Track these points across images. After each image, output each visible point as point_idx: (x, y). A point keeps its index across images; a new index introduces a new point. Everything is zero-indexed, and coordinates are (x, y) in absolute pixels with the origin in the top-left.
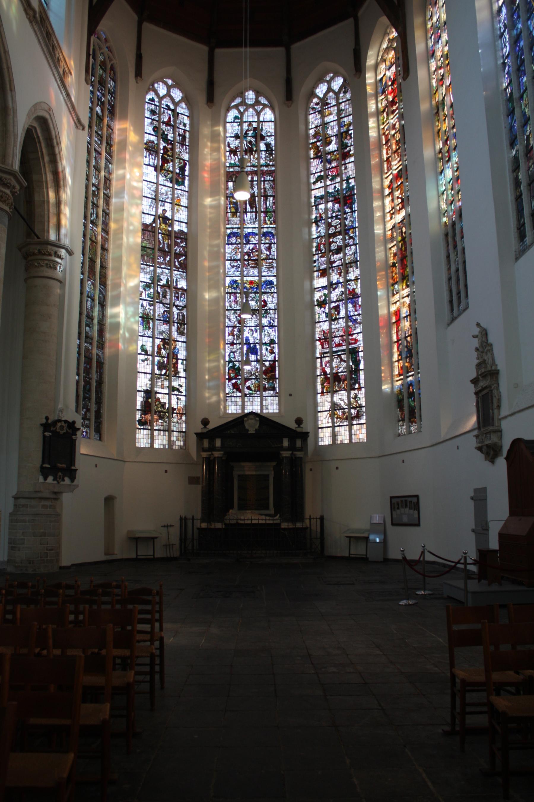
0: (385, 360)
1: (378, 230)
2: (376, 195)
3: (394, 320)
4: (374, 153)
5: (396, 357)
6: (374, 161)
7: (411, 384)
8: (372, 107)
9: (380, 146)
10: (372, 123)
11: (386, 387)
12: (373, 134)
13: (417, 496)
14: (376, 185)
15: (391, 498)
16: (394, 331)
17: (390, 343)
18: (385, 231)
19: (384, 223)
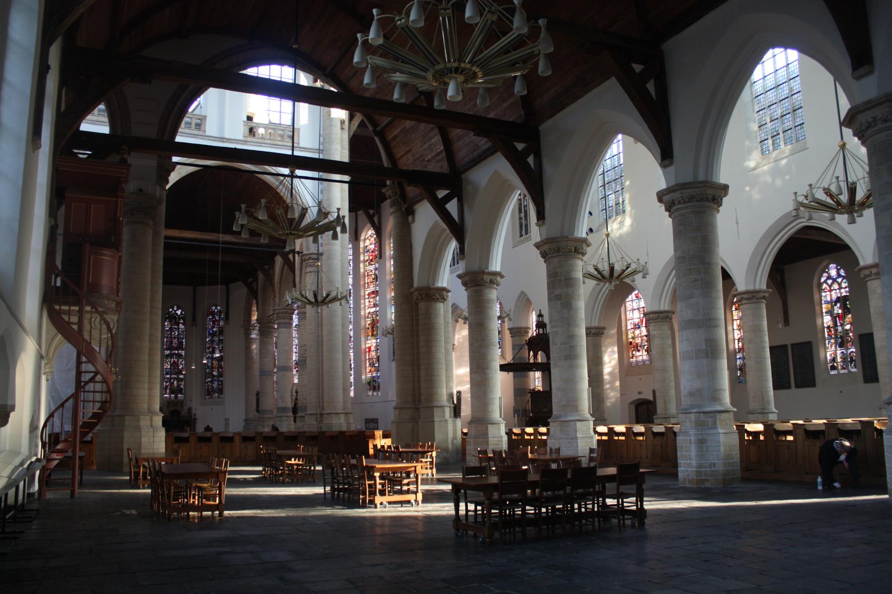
0: (363, 366)
1: (362, 313)
2: (362, 298)
3: (367, 350)
4: (362, 279)
5: (368, 365)
6: (362, 283)
7: (374, 377)
8: (362, 258)
9: (364, 276)
10: (362, 265)
11: (363, 377)
12: (362, 270)
13: (377, 419)
14: (362, 294)
15: (366, 419)
16: (367, 355)
17: (366, 360)
18: (365, 314)
19: (365, 310)
